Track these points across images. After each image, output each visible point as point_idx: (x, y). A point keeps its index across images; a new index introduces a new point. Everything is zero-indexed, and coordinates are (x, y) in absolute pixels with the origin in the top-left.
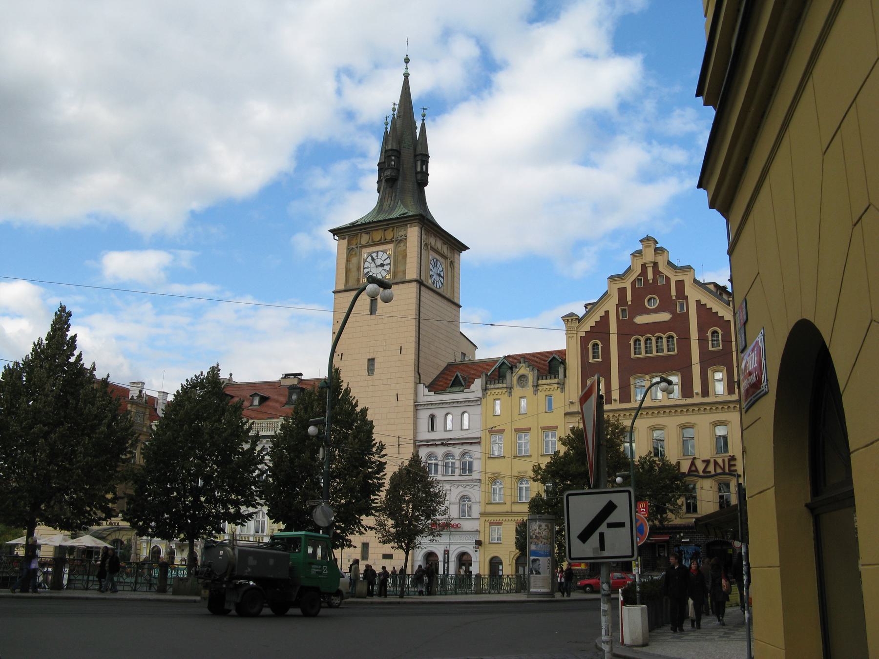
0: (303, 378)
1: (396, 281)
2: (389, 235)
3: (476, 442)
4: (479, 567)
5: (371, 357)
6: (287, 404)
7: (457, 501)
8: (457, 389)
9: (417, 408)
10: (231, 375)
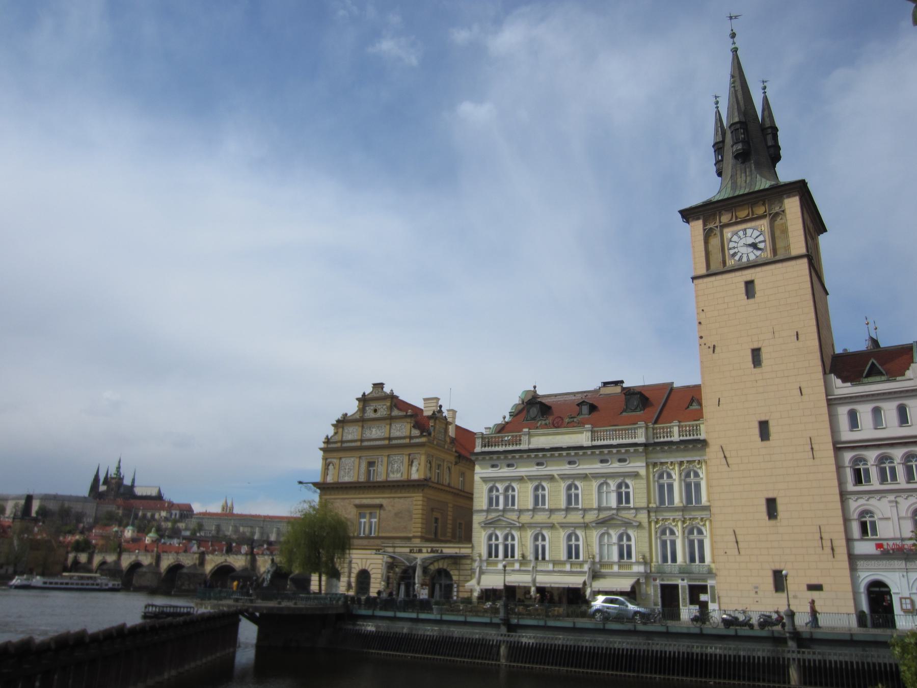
0: (624, 385)
1: (777, 258)
5: (756, 346)
6: (625, 411)
7: (909, 514)
8: (878, 378)
9: (832, 403)
10: (535, 387)
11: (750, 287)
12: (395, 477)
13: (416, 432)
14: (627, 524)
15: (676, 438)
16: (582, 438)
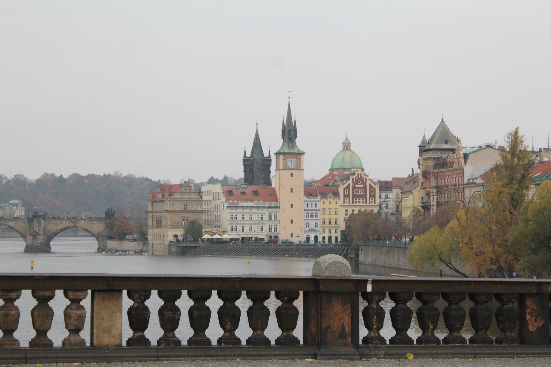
2: (295, 156)
3: (319, 210)
4: (320, 239)
11: (292, 174)
12: (194, 209)
13: (200, 197)
14: (263, 224)
15: (273, 206)
16: (253, 204)
